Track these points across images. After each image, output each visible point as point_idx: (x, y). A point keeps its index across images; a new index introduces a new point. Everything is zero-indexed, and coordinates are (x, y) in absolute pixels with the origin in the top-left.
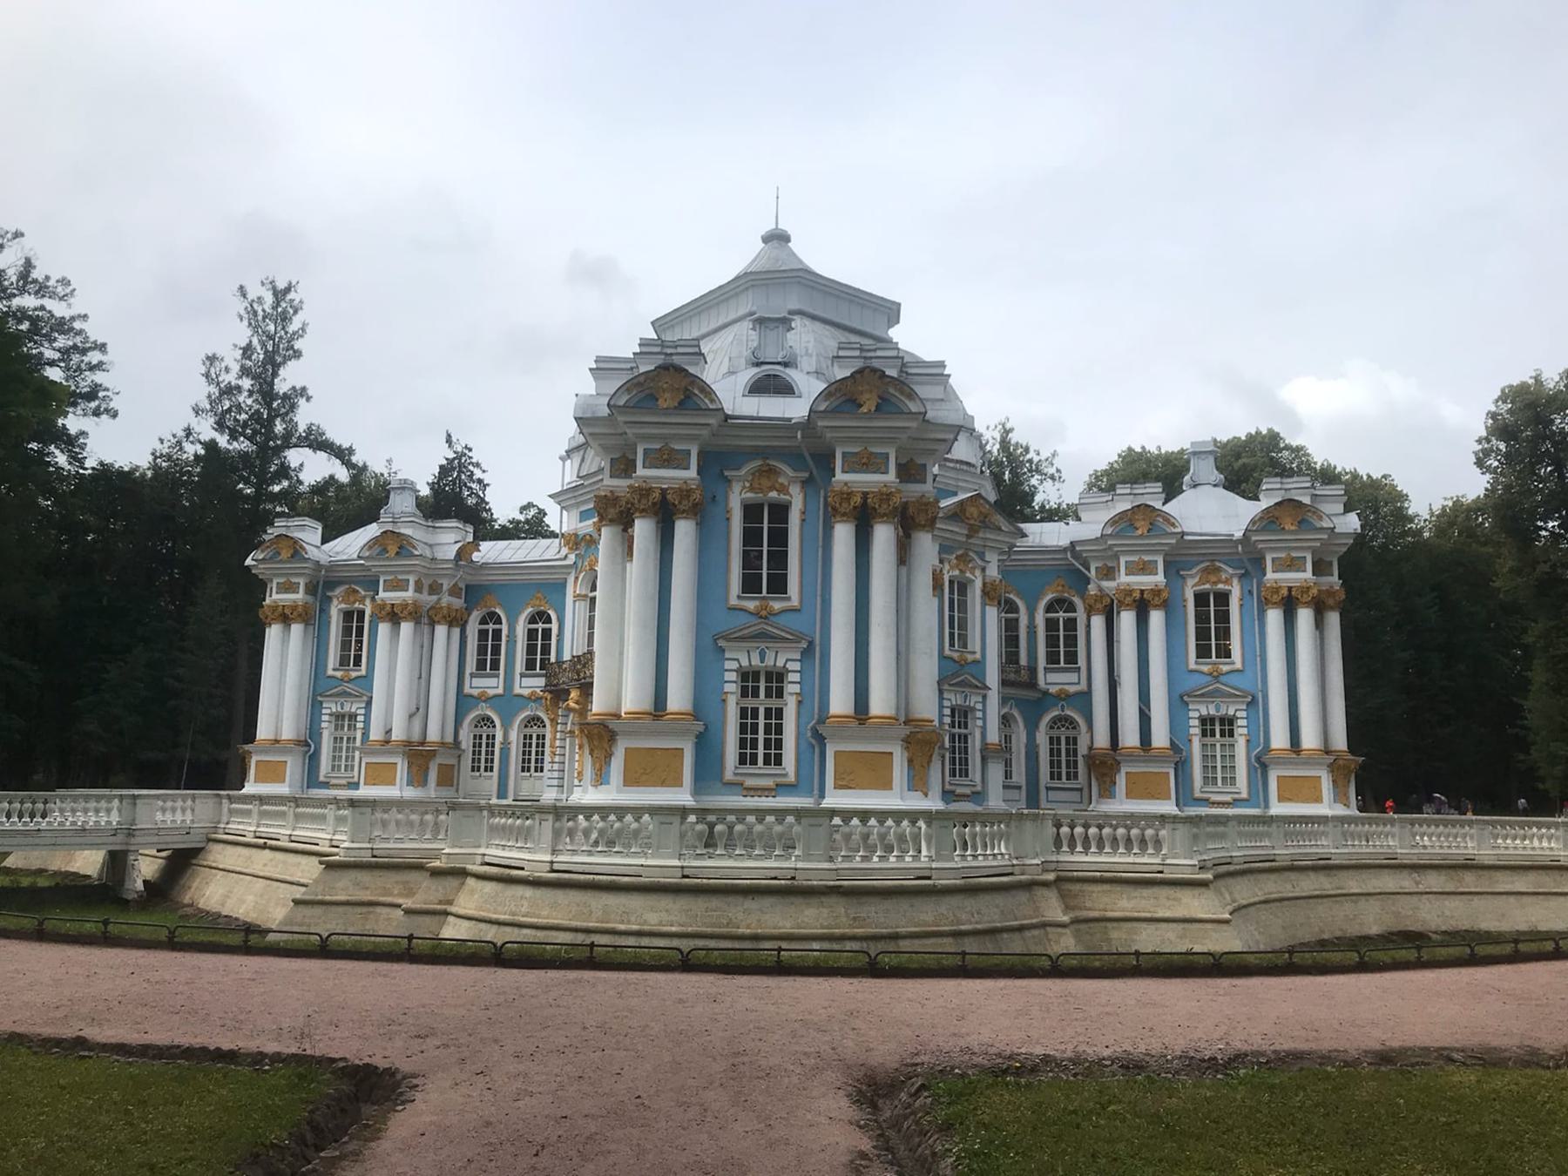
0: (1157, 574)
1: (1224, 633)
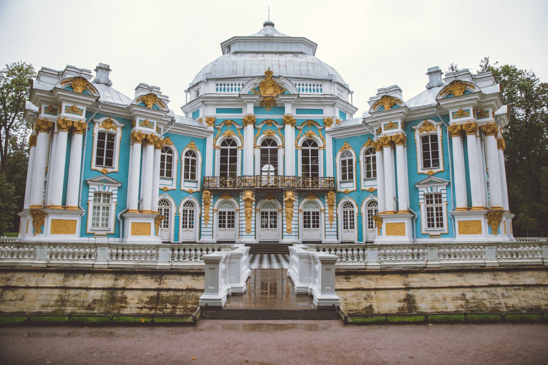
0: (398, 128)
1: (436, 155)
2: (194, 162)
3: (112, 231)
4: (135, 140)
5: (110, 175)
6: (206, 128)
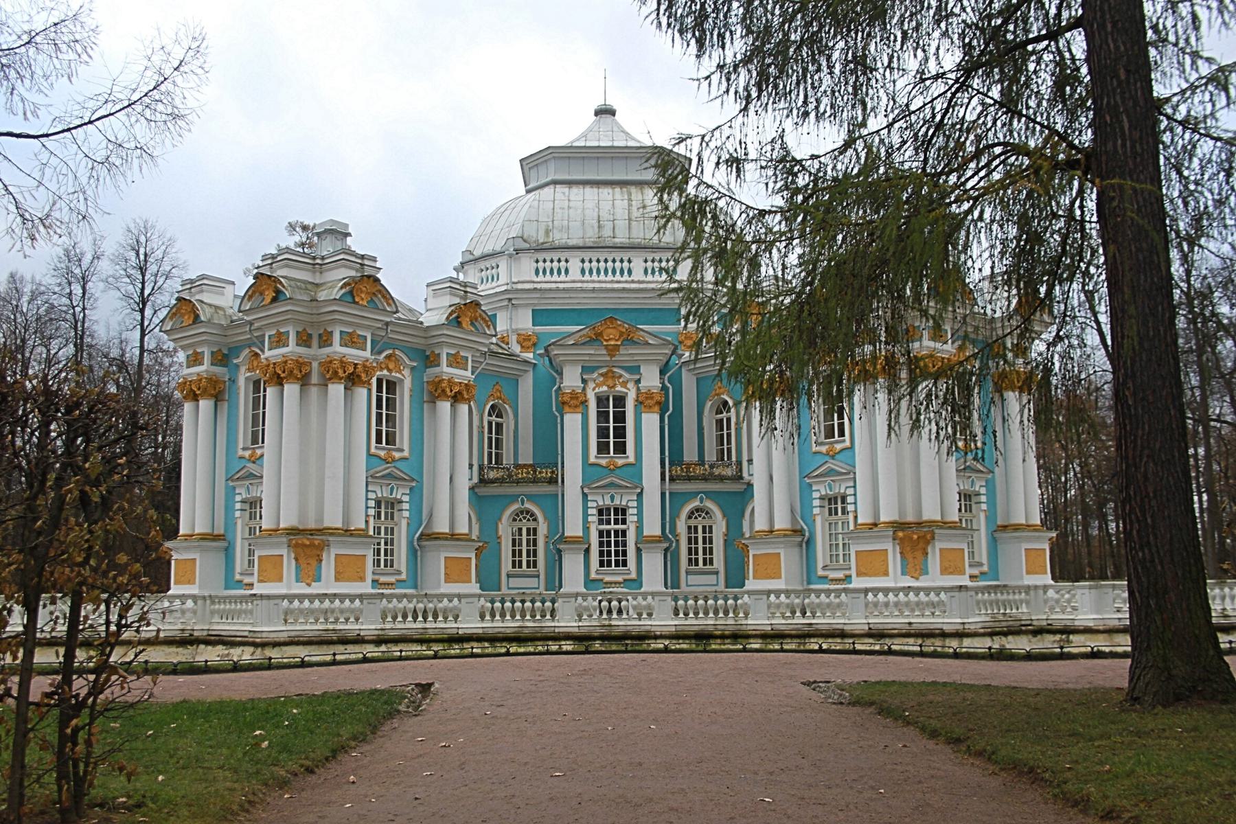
2: (499, 426)
3: (403, 576)
4: (443, 395)
5: (398, 464)
6: (518, 356)
